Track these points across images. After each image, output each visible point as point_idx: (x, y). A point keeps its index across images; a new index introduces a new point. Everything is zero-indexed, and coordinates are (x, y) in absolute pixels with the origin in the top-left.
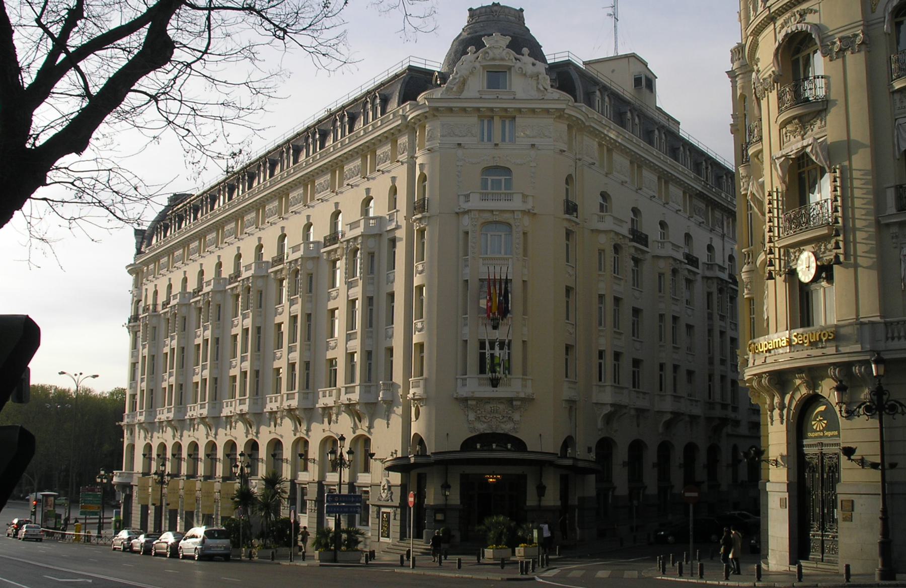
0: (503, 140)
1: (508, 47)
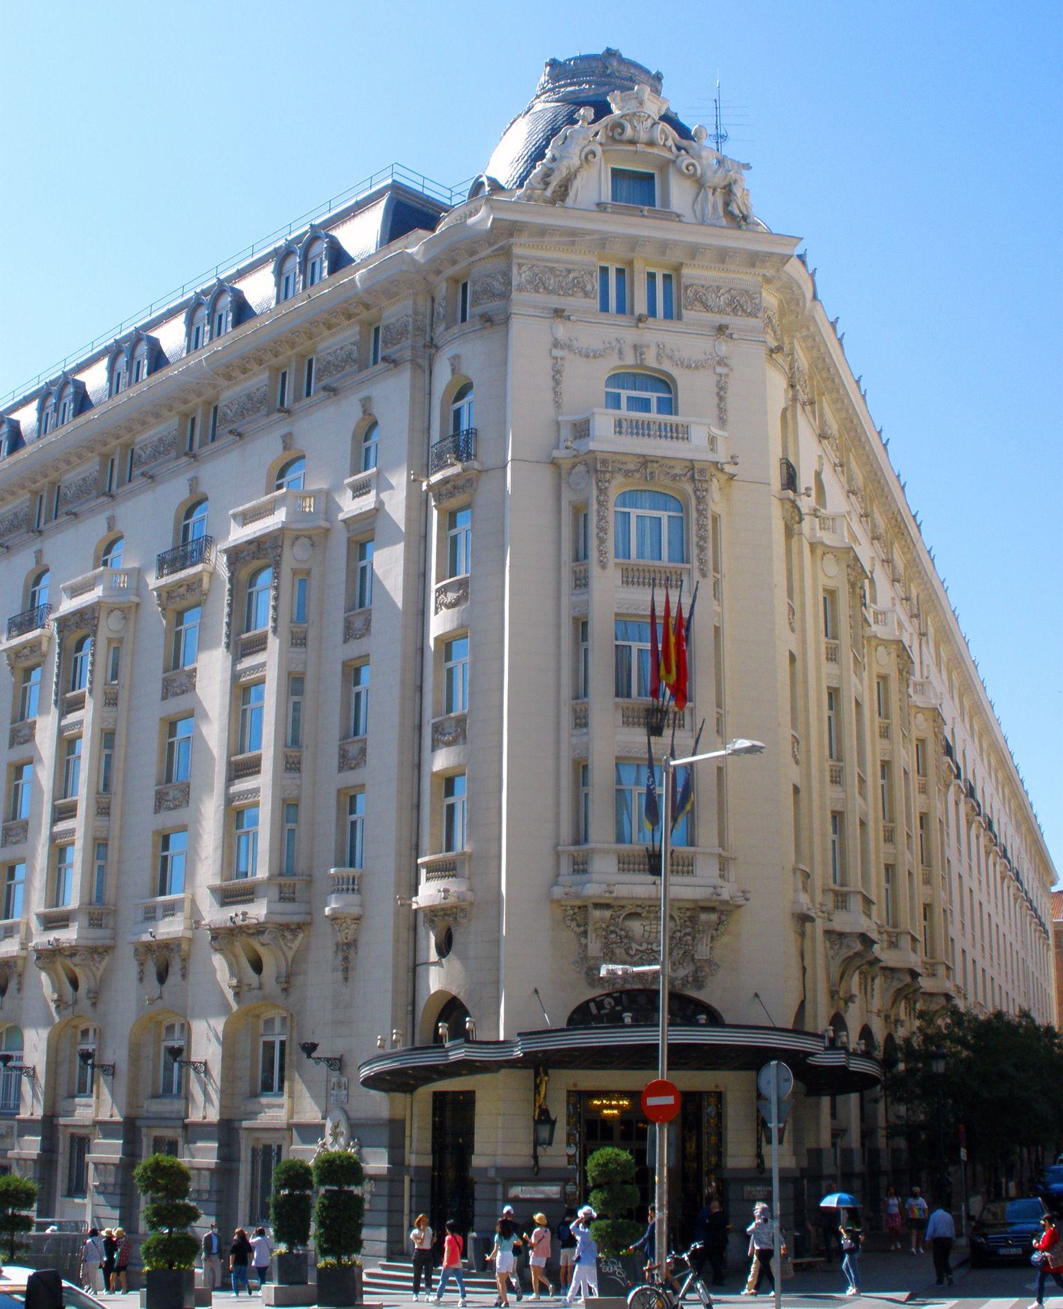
0: (652, 312)
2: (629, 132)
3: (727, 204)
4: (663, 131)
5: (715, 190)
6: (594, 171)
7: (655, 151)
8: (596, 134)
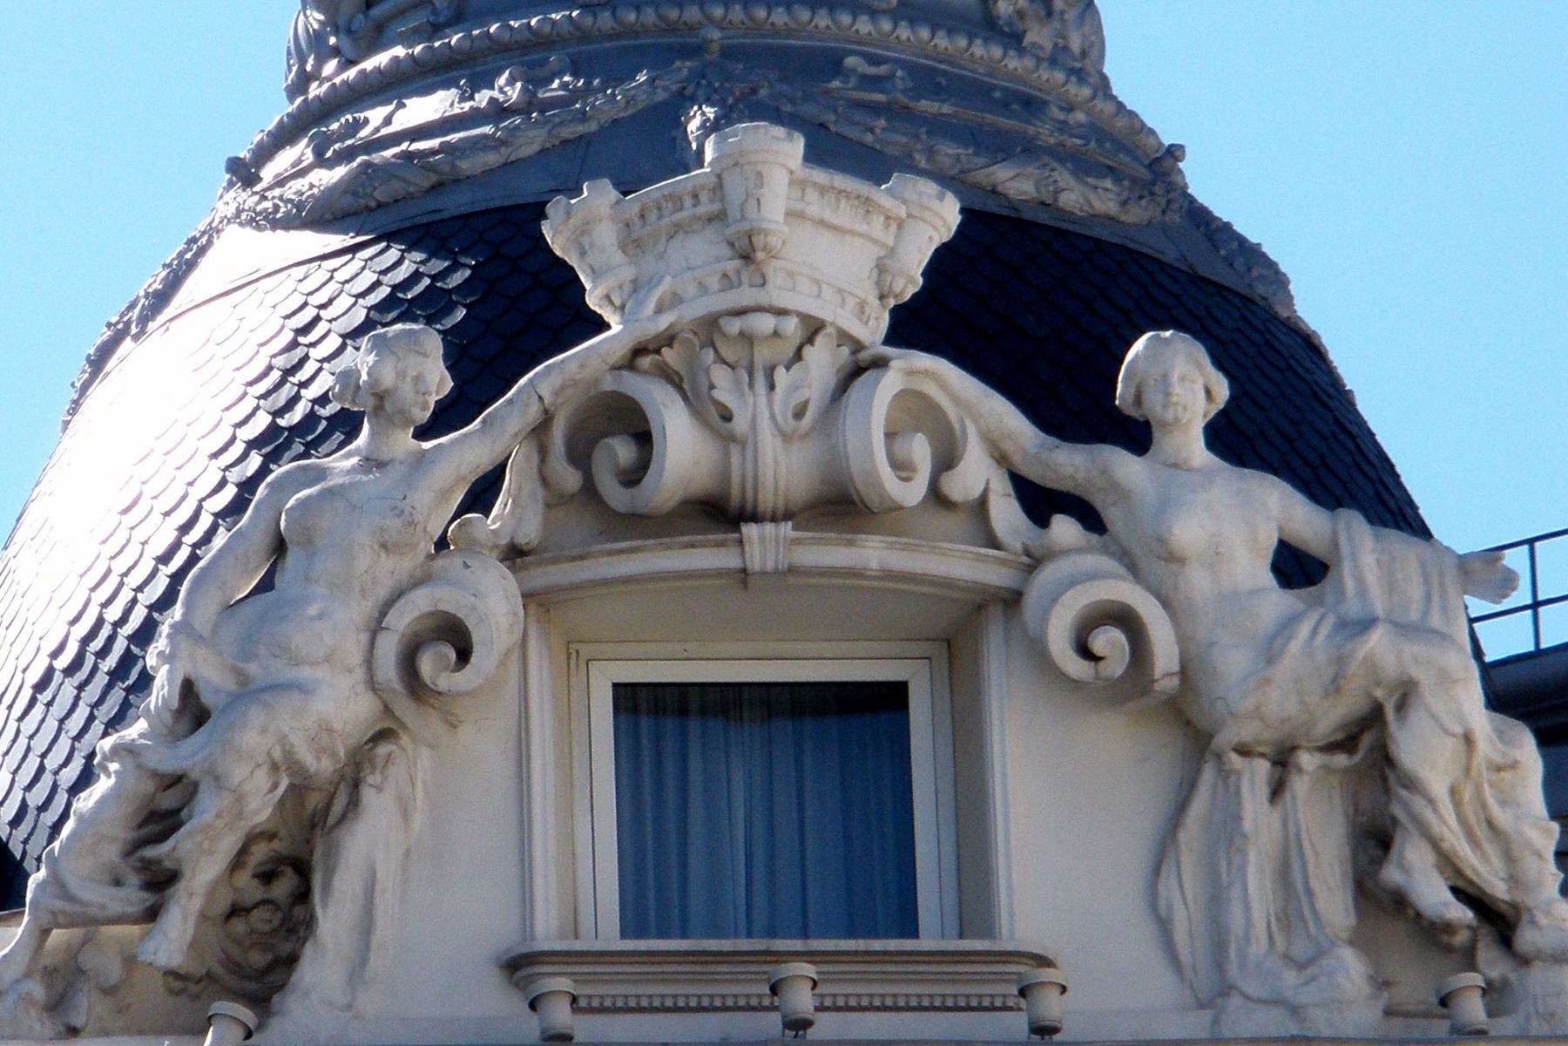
1: (913, 325)
2: (683, 453)
3: (1375, 839)
4: (917, 411)
5: (1283, 760)
6: (482, 744)
7: (872, 553)
8: (482, 494)
